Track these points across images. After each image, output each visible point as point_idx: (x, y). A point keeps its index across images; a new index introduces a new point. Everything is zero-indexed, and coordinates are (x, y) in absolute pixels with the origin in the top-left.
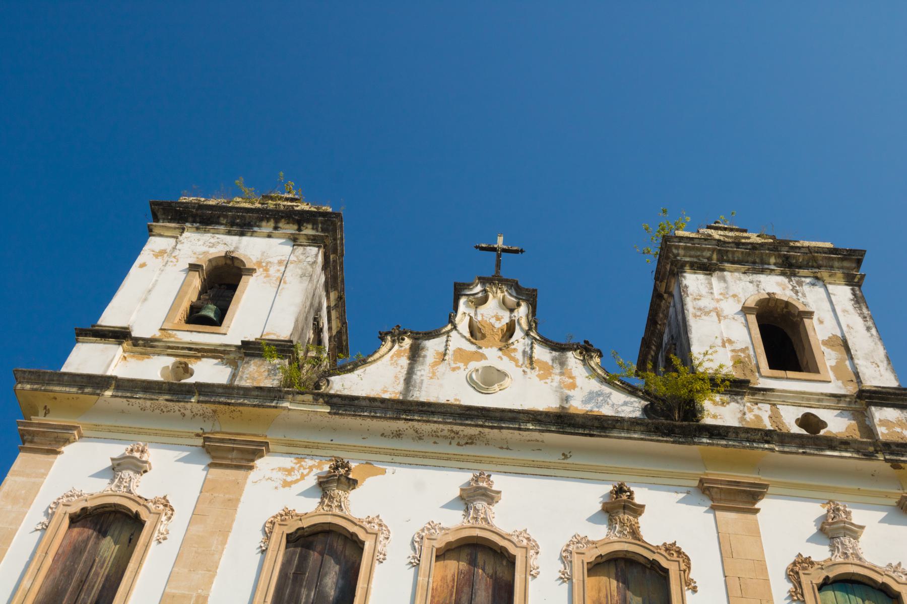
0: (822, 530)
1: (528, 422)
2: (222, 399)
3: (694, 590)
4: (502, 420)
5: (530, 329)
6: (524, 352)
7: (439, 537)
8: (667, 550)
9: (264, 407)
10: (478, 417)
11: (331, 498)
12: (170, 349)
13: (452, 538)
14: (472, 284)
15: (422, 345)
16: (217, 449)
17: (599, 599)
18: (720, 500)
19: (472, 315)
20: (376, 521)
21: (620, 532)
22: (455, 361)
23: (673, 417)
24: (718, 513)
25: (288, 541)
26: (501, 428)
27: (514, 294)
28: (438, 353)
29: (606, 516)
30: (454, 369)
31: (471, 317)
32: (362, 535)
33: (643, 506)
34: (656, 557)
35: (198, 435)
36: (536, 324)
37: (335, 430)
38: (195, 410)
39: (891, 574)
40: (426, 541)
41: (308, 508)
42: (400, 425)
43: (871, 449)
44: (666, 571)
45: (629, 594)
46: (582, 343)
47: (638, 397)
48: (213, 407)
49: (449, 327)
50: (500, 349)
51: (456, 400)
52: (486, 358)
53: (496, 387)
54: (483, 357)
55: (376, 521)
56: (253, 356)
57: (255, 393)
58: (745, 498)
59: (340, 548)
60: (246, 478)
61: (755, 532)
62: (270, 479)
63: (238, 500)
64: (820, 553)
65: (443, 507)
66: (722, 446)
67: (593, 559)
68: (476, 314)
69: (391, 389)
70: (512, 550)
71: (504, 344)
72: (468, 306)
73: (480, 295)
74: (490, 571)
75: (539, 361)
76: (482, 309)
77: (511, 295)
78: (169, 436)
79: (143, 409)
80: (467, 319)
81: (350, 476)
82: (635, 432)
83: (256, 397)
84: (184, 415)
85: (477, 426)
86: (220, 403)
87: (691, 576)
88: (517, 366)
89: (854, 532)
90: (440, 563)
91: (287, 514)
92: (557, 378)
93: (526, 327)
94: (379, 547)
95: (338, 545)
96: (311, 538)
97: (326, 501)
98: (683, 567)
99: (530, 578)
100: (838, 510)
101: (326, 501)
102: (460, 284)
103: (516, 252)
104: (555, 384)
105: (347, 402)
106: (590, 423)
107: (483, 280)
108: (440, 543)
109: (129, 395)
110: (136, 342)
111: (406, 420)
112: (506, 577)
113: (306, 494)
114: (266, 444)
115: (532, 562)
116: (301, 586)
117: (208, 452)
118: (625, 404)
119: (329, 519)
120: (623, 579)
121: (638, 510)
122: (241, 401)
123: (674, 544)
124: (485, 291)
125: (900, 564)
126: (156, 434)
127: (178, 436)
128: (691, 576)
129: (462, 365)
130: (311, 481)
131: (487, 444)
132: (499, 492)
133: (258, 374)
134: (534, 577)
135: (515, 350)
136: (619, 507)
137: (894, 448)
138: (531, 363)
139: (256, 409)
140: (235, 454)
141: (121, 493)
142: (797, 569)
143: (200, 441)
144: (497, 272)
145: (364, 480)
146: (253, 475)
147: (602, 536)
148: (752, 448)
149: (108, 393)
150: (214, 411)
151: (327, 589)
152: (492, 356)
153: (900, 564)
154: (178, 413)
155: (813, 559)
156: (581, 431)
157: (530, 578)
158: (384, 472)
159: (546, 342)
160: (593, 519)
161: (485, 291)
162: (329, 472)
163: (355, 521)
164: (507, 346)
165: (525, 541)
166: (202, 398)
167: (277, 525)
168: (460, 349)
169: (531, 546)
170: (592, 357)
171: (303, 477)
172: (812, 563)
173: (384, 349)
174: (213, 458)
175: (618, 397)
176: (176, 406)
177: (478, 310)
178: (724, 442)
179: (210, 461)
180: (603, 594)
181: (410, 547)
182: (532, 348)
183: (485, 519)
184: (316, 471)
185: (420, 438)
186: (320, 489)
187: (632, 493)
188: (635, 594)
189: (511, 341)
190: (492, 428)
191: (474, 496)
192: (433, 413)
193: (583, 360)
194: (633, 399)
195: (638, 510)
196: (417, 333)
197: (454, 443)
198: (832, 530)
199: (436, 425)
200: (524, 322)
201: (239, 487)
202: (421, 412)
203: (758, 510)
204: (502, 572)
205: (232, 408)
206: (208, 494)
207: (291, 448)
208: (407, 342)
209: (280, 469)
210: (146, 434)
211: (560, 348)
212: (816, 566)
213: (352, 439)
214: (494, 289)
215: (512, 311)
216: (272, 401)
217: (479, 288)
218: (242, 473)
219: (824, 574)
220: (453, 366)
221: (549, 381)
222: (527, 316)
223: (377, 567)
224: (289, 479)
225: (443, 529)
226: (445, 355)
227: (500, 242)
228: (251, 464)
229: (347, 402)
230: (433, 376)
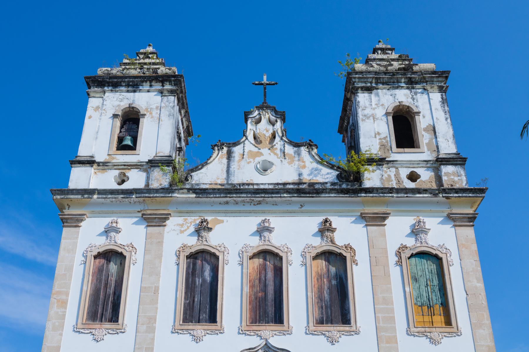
0: (412, 232)
1: (284, 193)
2: (147, 195)
3: (357, 264)
4: (273, 193)
5: (283, 136)
6: (281, 149)
7: (250, 251)
8: (346, 247)
9: (166, 197)
10: (262, 193)
11: (202, 237)
12: (116, 166)
13: (255, 251)
14: (253, 111)
15: (232, 150)
17: (318, 271)
18: (369, 222)
19: (255, 130)
20: (223, 246)
21: (326, 241)
22: (248, 158)
23: (350, 182)
24: (368, 227)
25: (187, 258)
26: (272, 197)
27: (274, 115)
28: (240, 154)
29: (320, 233)
30: (249, 163)
31: (254, 131)
32: (217, 253)
33: (336, 229)
34: (342, 251)
35: (139, 212)
36: (286, 132)
37: (199, 203)
38: (135, 200)
39: (440, 249)
40: (244, 253)
41: (193, 243)
42: (228, 199)
43: (437, 192)
44: (346, 257)
45: (330, 267)
46: (308, 142)
47: (334, 170)
48: (143, 199)
49: (244, 138)
50: (269, 149)
51: (251, 180)
52: (263, 155)
53: (269, 171)
54: (261, 154)
55: (223, 246)
56: (155, 166)
57: (161, 191)
58: (380, 219)
59: (209, 258)
60: (164, 231)
62: (174, 230)
63: (163, 242)
64: (410, 242)
65: (250, 236)
66: (371, 197)
67: (315, 255)
68: (256, 129)
69: (220, 177)
70: (281, 254)
71: (270, 146)
72: (252, 125)
73: (257, 117)
74: (273, 263)
75: (288, 154)
76: (259, 126)
77: (272, 115)
78: (126, 213)
79: (112, 202)
80: (252, 132)
81: (209, 226)
82: (332, 193)
83: (162, 193)
84: (130, 203)
85: (261, 197)
86: (146, 197)
87: (356, 258)
88: (278, 158)
89: (425, 232)
90: (252, 260)
91: (184, 247)
92: (297, 163)
93: (281, 135)
94: (225, 258)
95: (208, 257)
96: (196, 255)
97: (200, 238)
98: (352, 254)
99: (289, 265)
100: (420, 222)
101: (200, 238)
102: (247, 112)
103: (274, 84)
104: (296, 166)
105: (202, 191)
106: (312, 191)
107: (258, 108)
108: (251, 254)
109: (104, 196)
110: (99, 164)
111: (230, 197)
112: (279, 265)
113: (191, 235)
114: (170, 214)
115: (290, 258)
116: (195, 277)
117: (145, 219)
118: (328, 174)
119: (203, 247)
120: (328, 261)
121: (333, 230)
122: (155, 195)
123: (349, 244)
124: (259, 114)
125: (444, 244)
126: (120, 213)
128: (356, 258)
129: (252, 160)
130: (192, 229)
131: (267, 203)
132: (273, 228)
133: (160, 179)
134: (291, 265)
135: (276, 148)
136: (326, 229)
137: (447, 190)
138: (284, 156)
140: (157, 220)
141: (111, 244)
142: (400, 251)
143: (140, 215)
144: (265, 100)
145: (215, 226)
146: (166, 229)
147: (319, 244)
148: (384, 196)
149: (95, 196)
151: (206, 277)
152: (266, 154)
153: (444, 244)
155: (407, 246)
156: (308, 195)
157: (289, 265)
158: (222, 222)
159: (291, 143)
160: (314, 235)
161: (259, 114)
162: (199, 225)
163: (214, 247)
164: (272, 147)
165: (286, 249)
167: (181, 252)
168: (250, 151)
169: (289, 251)
170: (313, 149)
171: (188, 227)
172: (407, 248)
173: (215, 155)
174: (148, 222)
175: (325, 170)
176: (127, 200)
177: (257, 126)
178: (371, 195)
179: (146, 224)
180: (319, 269)
181: (238, 256)
182: (284, 147)
183: (269, 241)
184: (193, 224)
185: (237, 204)
186: (196, 233)
187: (331, 222)
188: (333, 266)
189: (274, 144)
190: (269, 197)
191: (263, 230)
192: (242, 193)
193: (309, 152)
194: (332, 171)
195: (333, 230)
196: (229, 144)
197: (252, 204)
198: (417, 231)
199: (243, 199)
200: (280, 132)
201: (161, 235)
202: (236, 193)
203: (386, 225)
204: (278, 263)
206: (149, 240)
207: (180, 213)
208: (225, 149)
209: (178, 225)
211: (297, 145)
212: (409, 249)
214: (264, 113)
215: (273, 125)
216: (169, 194)
217: (257, 112)
218: (162, 228)
219: (412, 252)
220: (248, 161)
221: (293, 165)
222: (281, 128)
223: (225, 266)
224: (182, 229)
225: (251, 247)
226: (243, 155)
227: (265, 80)
228: (164, 224)
229: (202, 191)
230: (239, 168)
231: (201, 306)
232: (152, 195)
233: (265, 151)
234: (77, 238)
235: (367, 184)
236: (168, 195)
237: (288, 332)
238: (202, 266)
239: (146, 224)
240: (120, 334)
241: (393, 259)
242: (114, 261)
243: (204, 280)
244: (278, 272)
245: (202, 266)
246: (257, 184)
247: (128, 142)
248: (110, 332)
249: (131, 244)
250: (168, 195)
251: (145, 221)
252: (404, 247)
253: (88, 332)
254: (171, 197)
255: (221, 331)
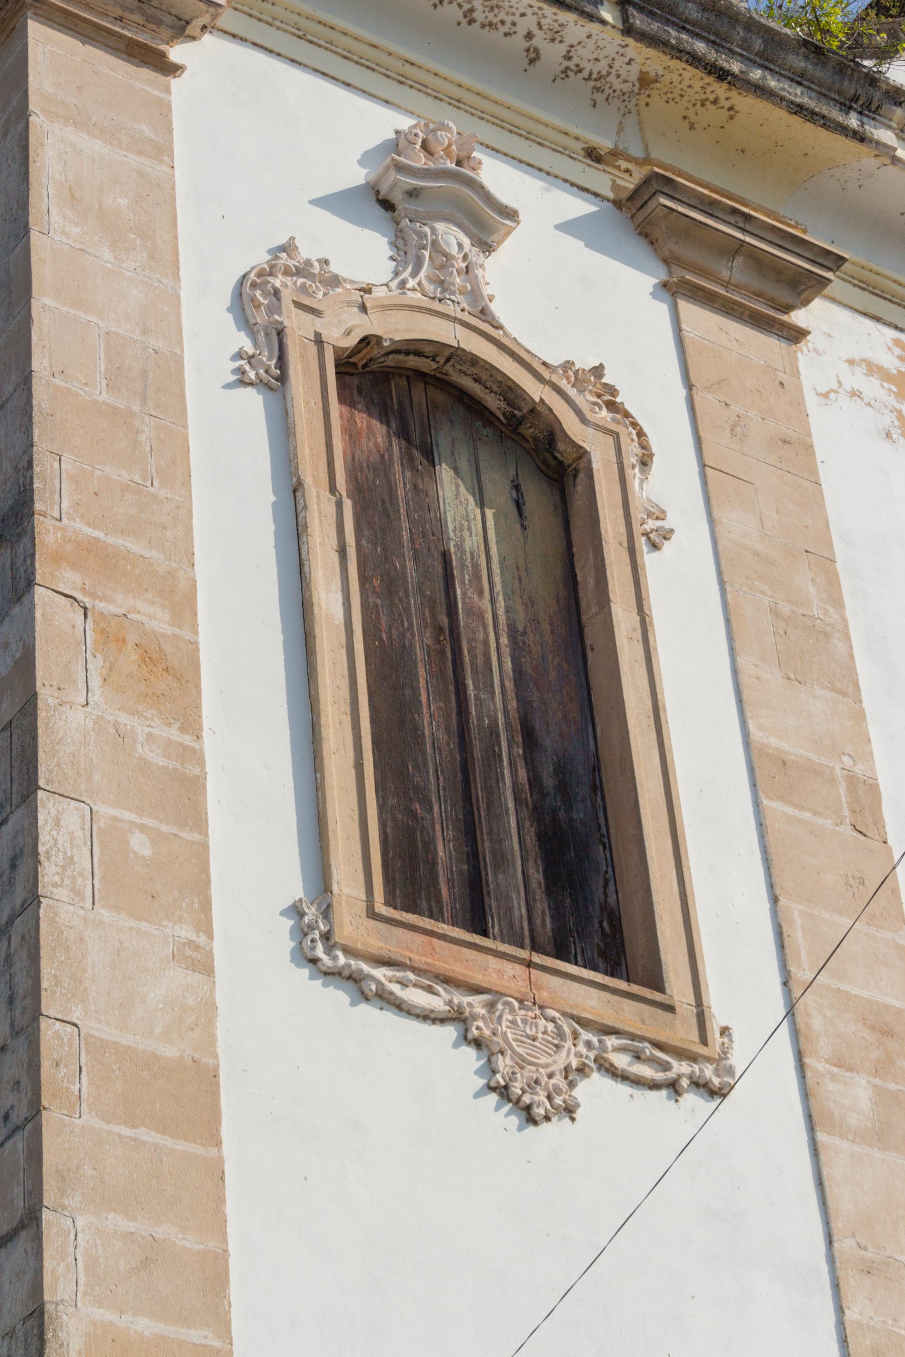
2: (700, 47)
16: (691, 232)
35: (593, 155)
83: (798, 79)
84: (534, 56)
122: (756, 74)
127: (529, 136)
139: (796, 121)
140: (736, 270)
141: (449, 308)
150: (645, 81)
154: (519, 42)
166: (638, 20)
174: (668, 261)
205: (720, 90)
210: (422, 88)
216: (847, 108)
232: (736, 67)
234: (163, 151)
236: (836, 114)
239: (662, 274)
240: (691, 1099)
242: (464, 464)
248: (621, 1061)
249: (598, 371)
250: (836, 114)
251: (640, 249)
253: (436, 1003)
254: (860, 137)
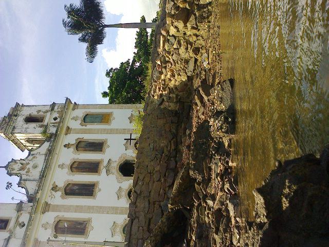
41: (59, 193)
61: (75, 129)
64: (79, 122)
213: (48, 185)
231: (87, 190)
233: (28, 167)
235: (54, 132)
237: (102, 161)
238: (73, 190)
241: (84, 127)
243: (77, 189)
244: (80, 163)
245: (73, 190)
246: (42, 169)
247: (4, 224)
252: (81, 124)
255: (98, 182)
